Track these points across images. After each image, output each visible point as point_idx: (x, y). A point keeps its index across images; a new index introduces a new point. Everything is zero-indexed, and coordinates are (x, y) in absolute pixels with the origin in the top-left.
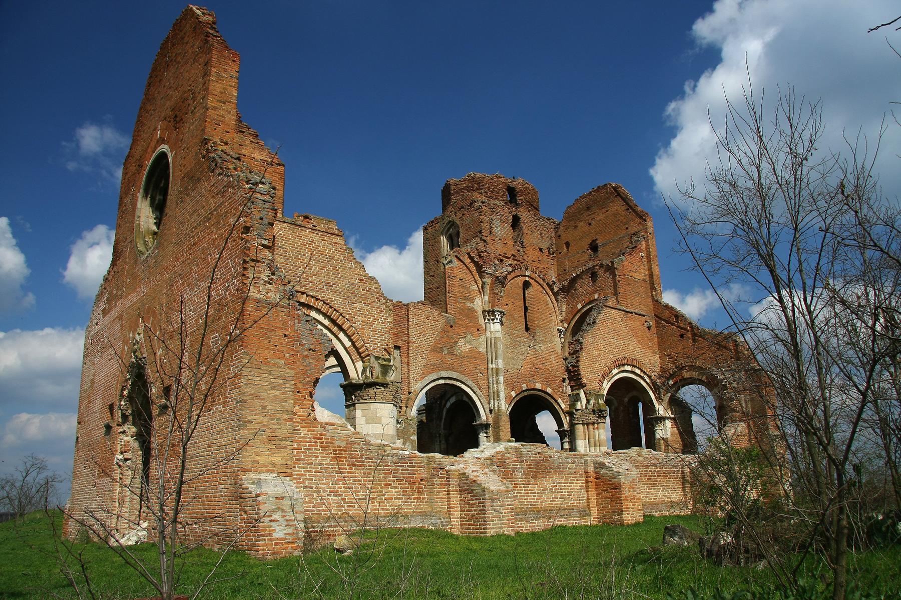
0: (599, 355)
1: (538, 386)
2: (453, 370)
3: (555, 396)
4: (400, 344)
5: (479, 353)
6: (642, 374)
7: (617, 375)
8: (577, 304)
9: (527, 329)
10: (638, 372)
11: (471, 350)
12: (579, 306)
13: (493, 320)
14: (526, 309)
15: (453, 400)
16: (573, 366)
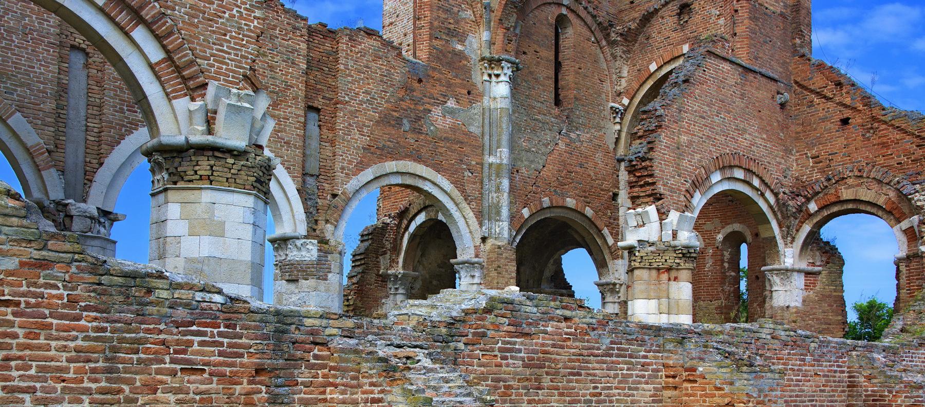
0: (690, 143)
1: (570, 202)
2: (419, 159)
3: (598, 223)
4: (319, 103)
5: (469, 134)
6: (762, 188)
7: (718, 184)
8: (650, 62)
9: (558, 102)
10: (756, 182)
11: (454, 129)
12: (653, 67)
13: (497, 76)
14: (558, 65)
15: (421, 218)
16: (643, 159)
